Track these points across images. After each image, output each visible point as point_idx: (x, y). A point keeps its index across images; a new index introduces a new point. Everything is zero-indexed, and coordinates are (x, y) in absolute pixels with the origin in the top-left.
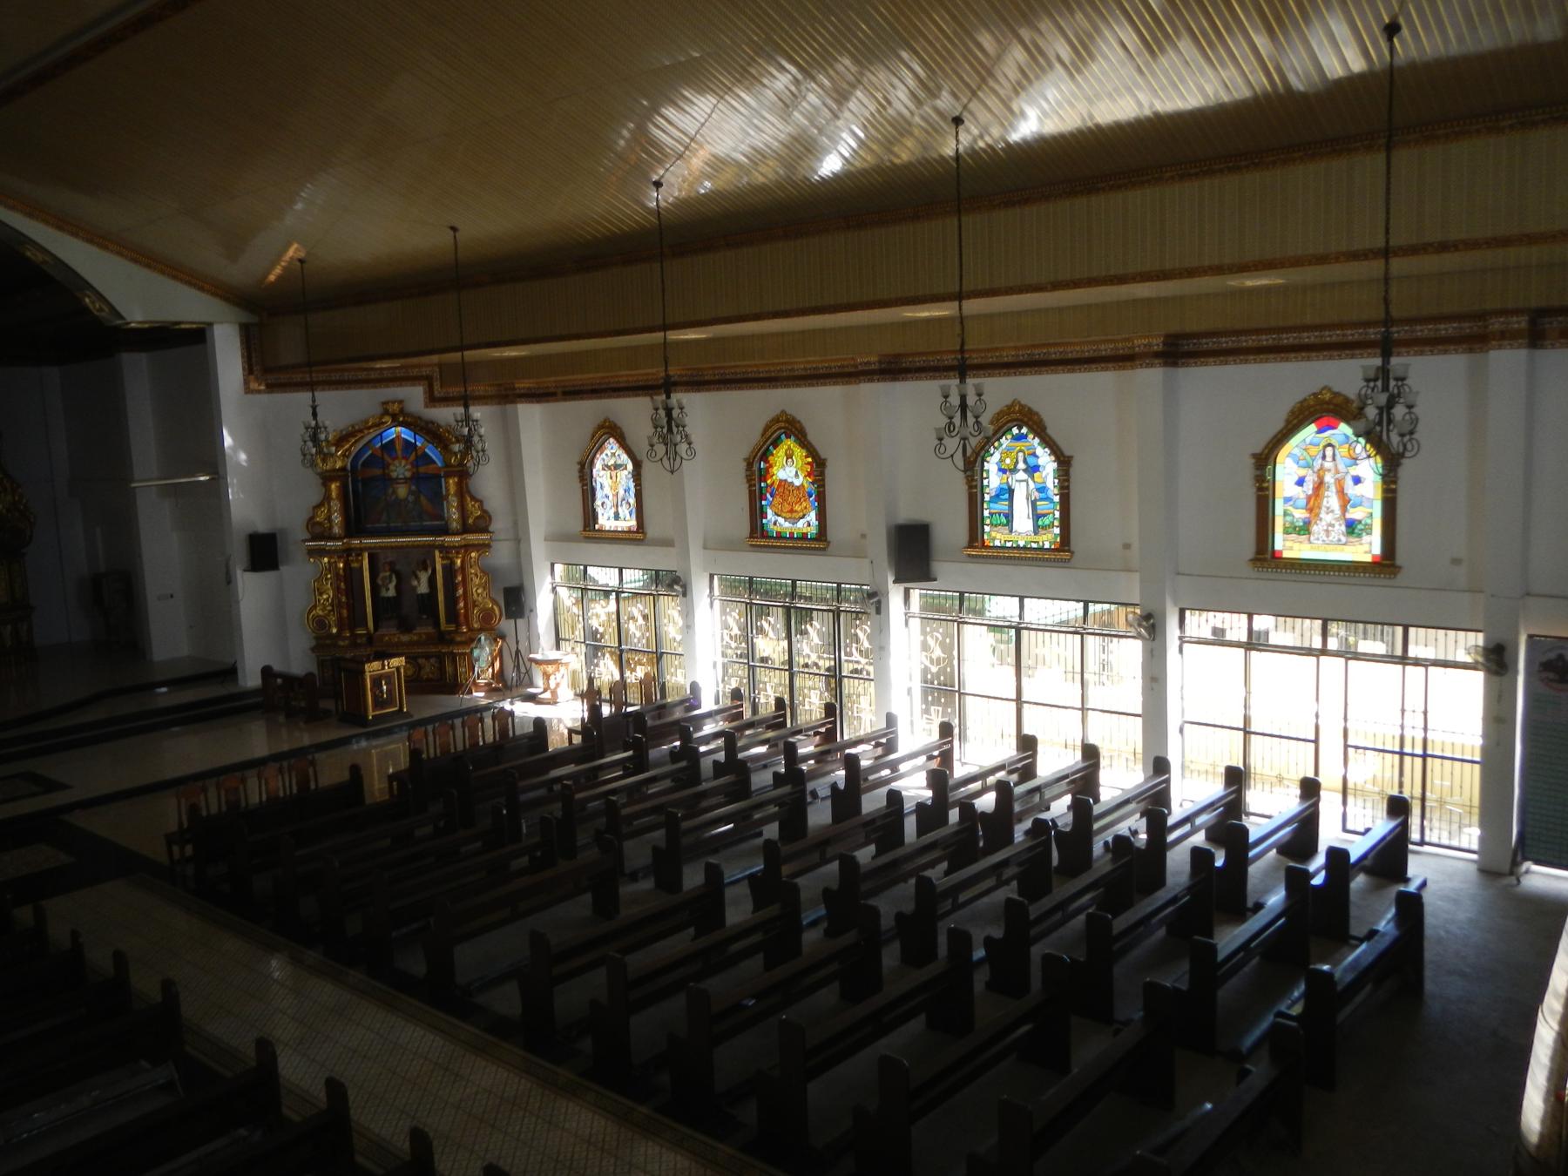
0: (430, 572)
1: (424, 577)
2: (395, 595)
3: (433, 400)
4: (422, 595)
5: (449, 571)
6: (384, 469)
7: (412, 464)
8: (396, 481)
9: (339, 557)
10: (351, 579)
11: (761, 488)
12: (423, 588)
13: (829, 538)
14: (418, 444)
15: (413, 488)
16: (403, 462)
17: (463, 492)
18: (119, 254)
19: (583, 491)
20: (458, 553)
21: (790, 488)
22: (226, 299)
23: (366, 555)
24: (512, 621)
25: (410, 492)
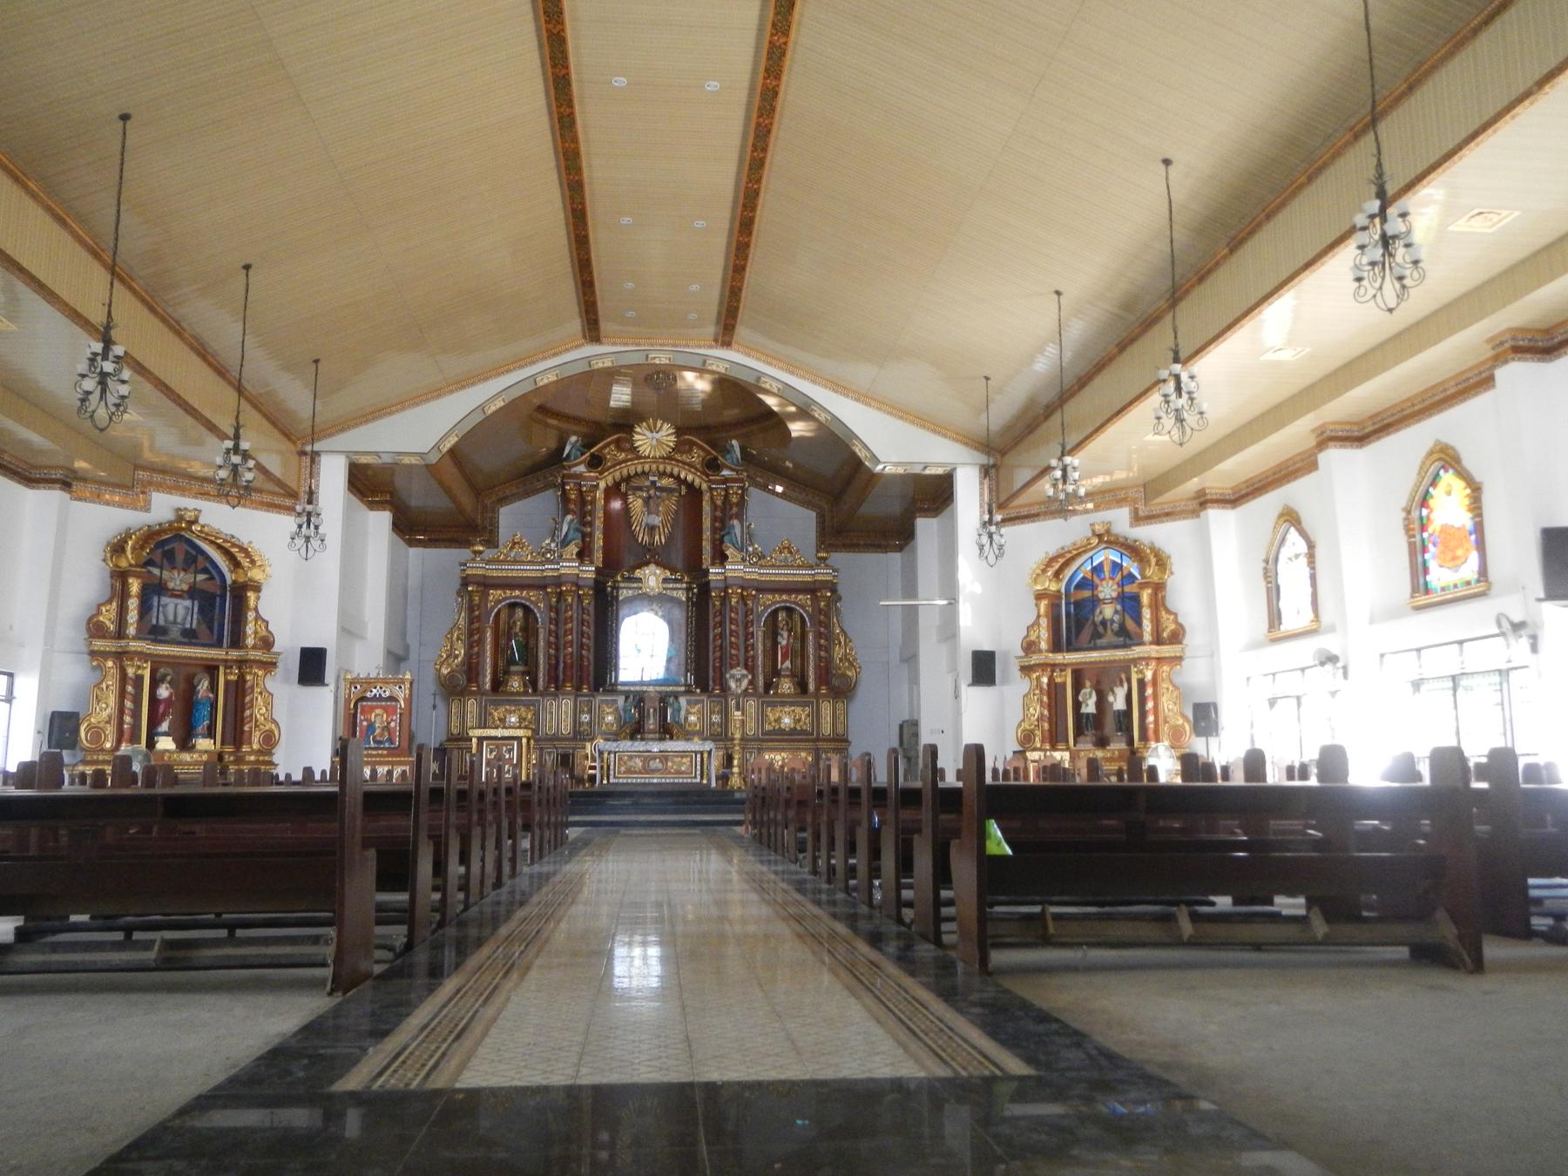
0: (1126, 685)
1: (1121, 693)
2: (1095, 712)
3: (1137, 519)
4: (1118, 711)
5: (1142, 684)
6: (1093, 590)
7: (1118, 584)
8: (1103, 601)
9: (1043, 670)
10: (1055, 691)
11: (1423, 540)
12: (1119, 703)
13: (1490, 580)
14: (1124, 564)
15: (1119, 607)
16: (1111, 582)
17: (1158, 604)
18: (879, 409)
19: (1268, 590)
20: (1147, 664)
21: (1451, 532)
22: (966, 444)
23: (1069, 672)
24: (1204, 739)
25: (1116, 612)
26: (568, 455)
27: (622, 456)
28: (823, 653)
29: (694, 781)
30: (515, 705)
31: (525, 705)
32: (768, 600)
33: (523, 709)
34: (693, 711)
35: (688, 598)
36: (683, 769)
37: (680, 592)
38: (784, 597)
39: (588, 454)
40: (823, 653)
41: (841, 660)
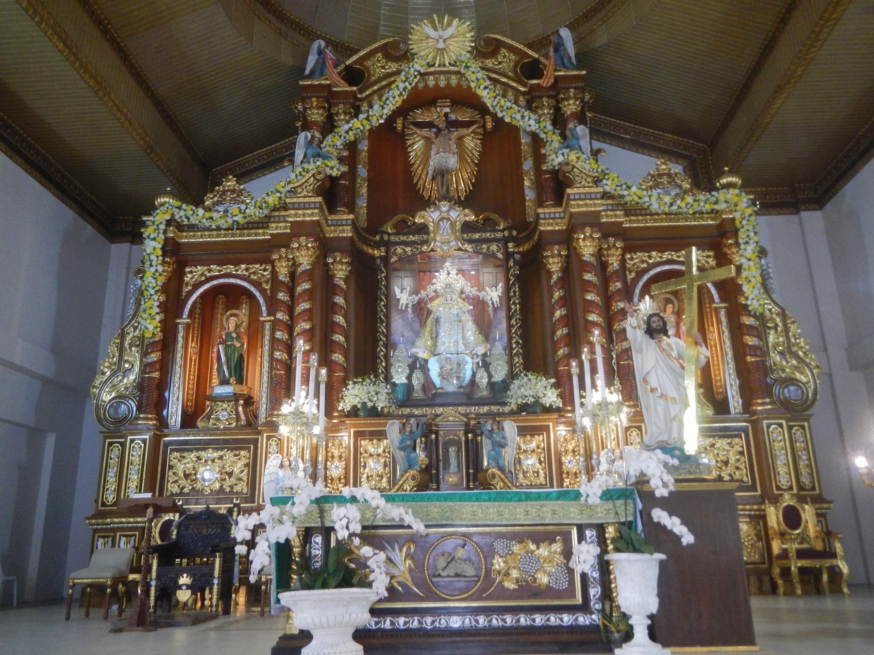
26: (311, 70)
27: (393, 67)
28: (750, 341)
29: (583, 620)
30: (217, 449)
31: (232, 449)
32: (643, 262)
33: (229, 455)
34: (533, 445)
35: (508, 255)
36: (543, 579)
37: (494, 247)
38: (666, 256)
39: (343, 66)
40: (750, 341)
41: (781, 353)
